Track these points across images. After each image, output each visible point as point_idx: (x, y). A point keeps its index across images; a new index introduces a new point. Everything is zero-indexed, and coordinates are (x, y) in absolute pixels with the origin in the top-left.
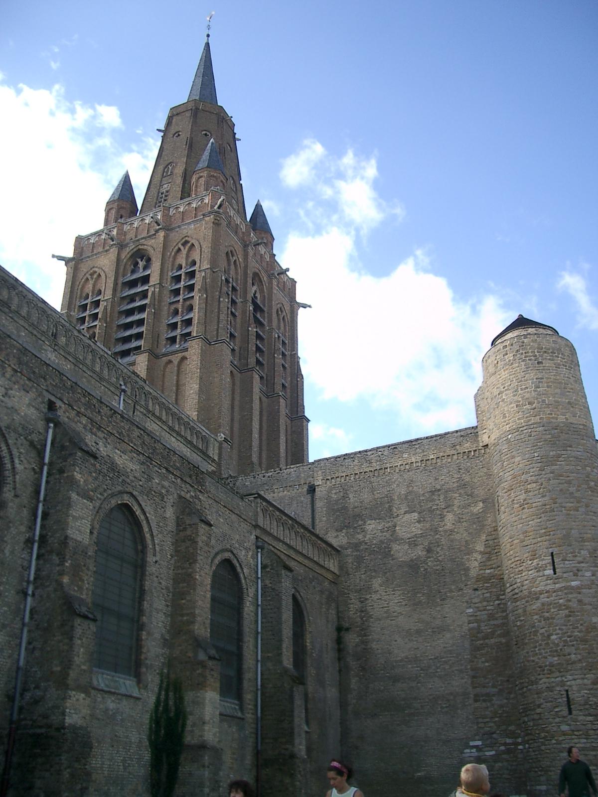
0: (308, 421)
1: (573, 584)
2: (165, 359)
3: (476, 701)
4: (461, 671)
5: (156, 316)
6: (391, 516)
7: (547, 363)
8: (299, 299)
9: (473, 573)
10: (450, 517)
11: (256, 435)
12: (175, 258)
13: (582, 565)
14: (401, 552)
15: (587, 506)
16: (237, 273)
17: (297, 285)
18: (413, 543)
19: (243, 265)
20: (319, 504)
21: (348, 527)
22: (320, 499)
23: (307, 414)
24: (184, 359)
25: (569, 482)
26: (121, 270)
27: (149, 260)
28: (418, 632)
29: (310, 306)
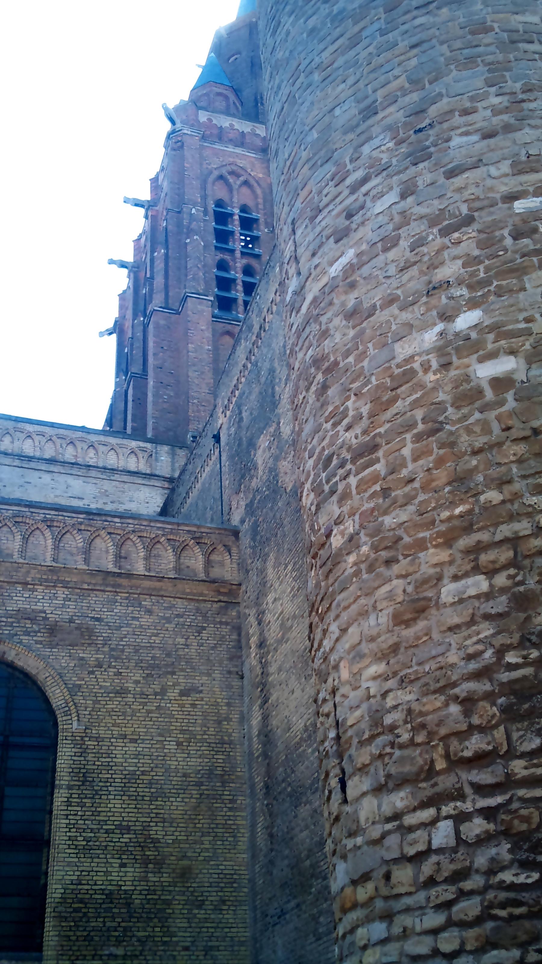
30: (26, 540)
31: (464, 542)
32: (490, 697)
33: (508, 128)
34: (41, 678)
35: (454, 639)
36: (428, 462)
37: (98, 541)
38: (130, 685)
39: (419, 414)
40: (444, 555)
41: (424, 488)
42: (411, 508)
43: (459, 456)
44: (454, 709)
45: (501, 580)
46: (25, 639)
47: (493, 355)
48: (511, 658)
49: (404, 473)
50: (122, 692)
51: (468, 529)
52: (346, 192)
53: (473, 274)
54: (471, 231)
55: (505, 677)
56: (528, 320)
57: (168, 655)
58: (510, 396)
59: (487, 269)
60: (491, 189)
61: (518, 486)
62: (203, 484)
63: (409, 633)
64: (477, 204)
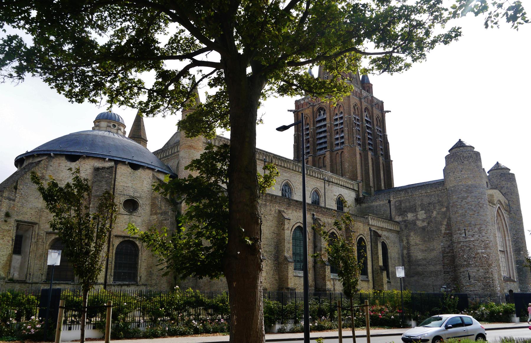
0: (392, 161)
1: (472, 239)
2: (336, 152)
3: (444, 273)
4: (439, 264)
5: (331, 135)
6: (416, 211)
7: (466, 162)
8: (385, 109)
9: (443, 232)
10: (435, 213)
11: (371, 175)
12: (334, 111)
14: (419, 224)
15: (478, 213)
16: (358, 112)
17: (384, 104)
18: (423, 221)
19: (360, 108)
20: (392, 207)
21: (402, 215)
22: (393, 205)
23: (391, 159)
24: (342, 152)
25: (471, 205)
26: (315, 116)
27: (324, 111)
28: (426, 250)
29: (390, 111)
62: (380, 204)
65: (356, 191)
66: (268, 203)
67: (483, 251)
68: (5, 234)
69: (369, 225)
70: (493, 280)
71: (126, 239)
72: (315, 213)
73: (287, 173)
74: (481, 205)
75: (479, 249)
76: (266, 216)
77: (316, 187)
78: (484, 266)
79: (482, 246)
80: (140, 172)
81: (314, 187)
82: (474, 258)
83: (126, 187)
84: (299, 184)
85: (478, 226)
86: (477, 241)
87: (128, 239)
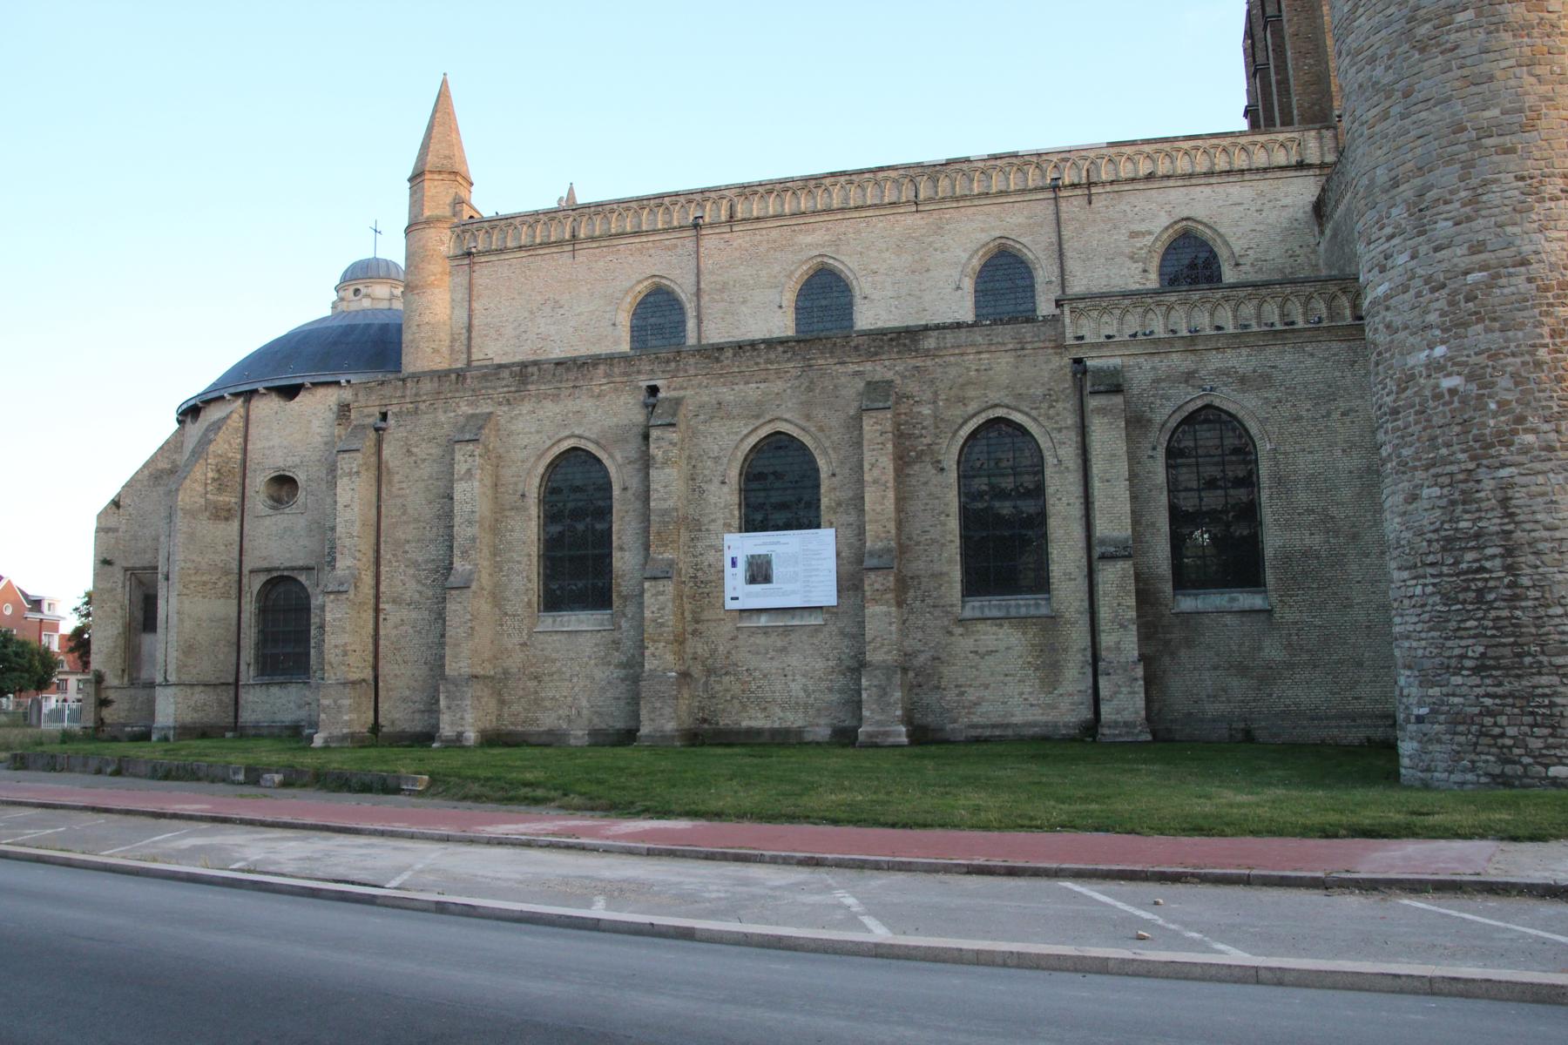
13: (1395, 241)
30: (1212, 315)
31: (1433, 471)
32: (1437, 540)
33: (1469, 219)
34: (1240, 416)
35: (1425, 514)
36: (1419, 427)
37: (1265, 305)
38: (1304, 413)
39: (1417, 400)
40: (1424, 475)
41: (1418, 439)
42: (1413, 449)
43: (1433, 427)
44: (1425, 544)
45: (1445, 491)
46: (1224, 389)
47: (1449, 375)
48: (1446, 526)
49: (1410, 430)
50: (1298, 419)
51: (1434, 465)
52: (1383, 239)
53: (1444, 323)
54: (1444, 292)
55: (1443, 533)
56: (1468, 356)
57: (1330, 387)
58: (1456, 399)
59: (1451, 321)
60: (1456, 265)
61: (1456, 448)
63: (1411, 507)
64: (1449, 275)
65: (1322, 166)
66: (422, 406)
67: (1440, 351)
68: (105, 597)
69: (1060, 346)
70: (1509, 552)
71: (275, 574)
72: (658, 383)
73: (814, 230)
74: (1424, 30)
75: (1413, 349)
76: (414, 450)
77: (998, 234)
78: (1445, 461)
79: (1433, 318)
80: (302, 398)
81: (984, 237)
82: (1395, 412)
83: (269, 448)
84: (887, 255)
85: (1406, 191)
86: (1406, 289)
87: (279, 573)
